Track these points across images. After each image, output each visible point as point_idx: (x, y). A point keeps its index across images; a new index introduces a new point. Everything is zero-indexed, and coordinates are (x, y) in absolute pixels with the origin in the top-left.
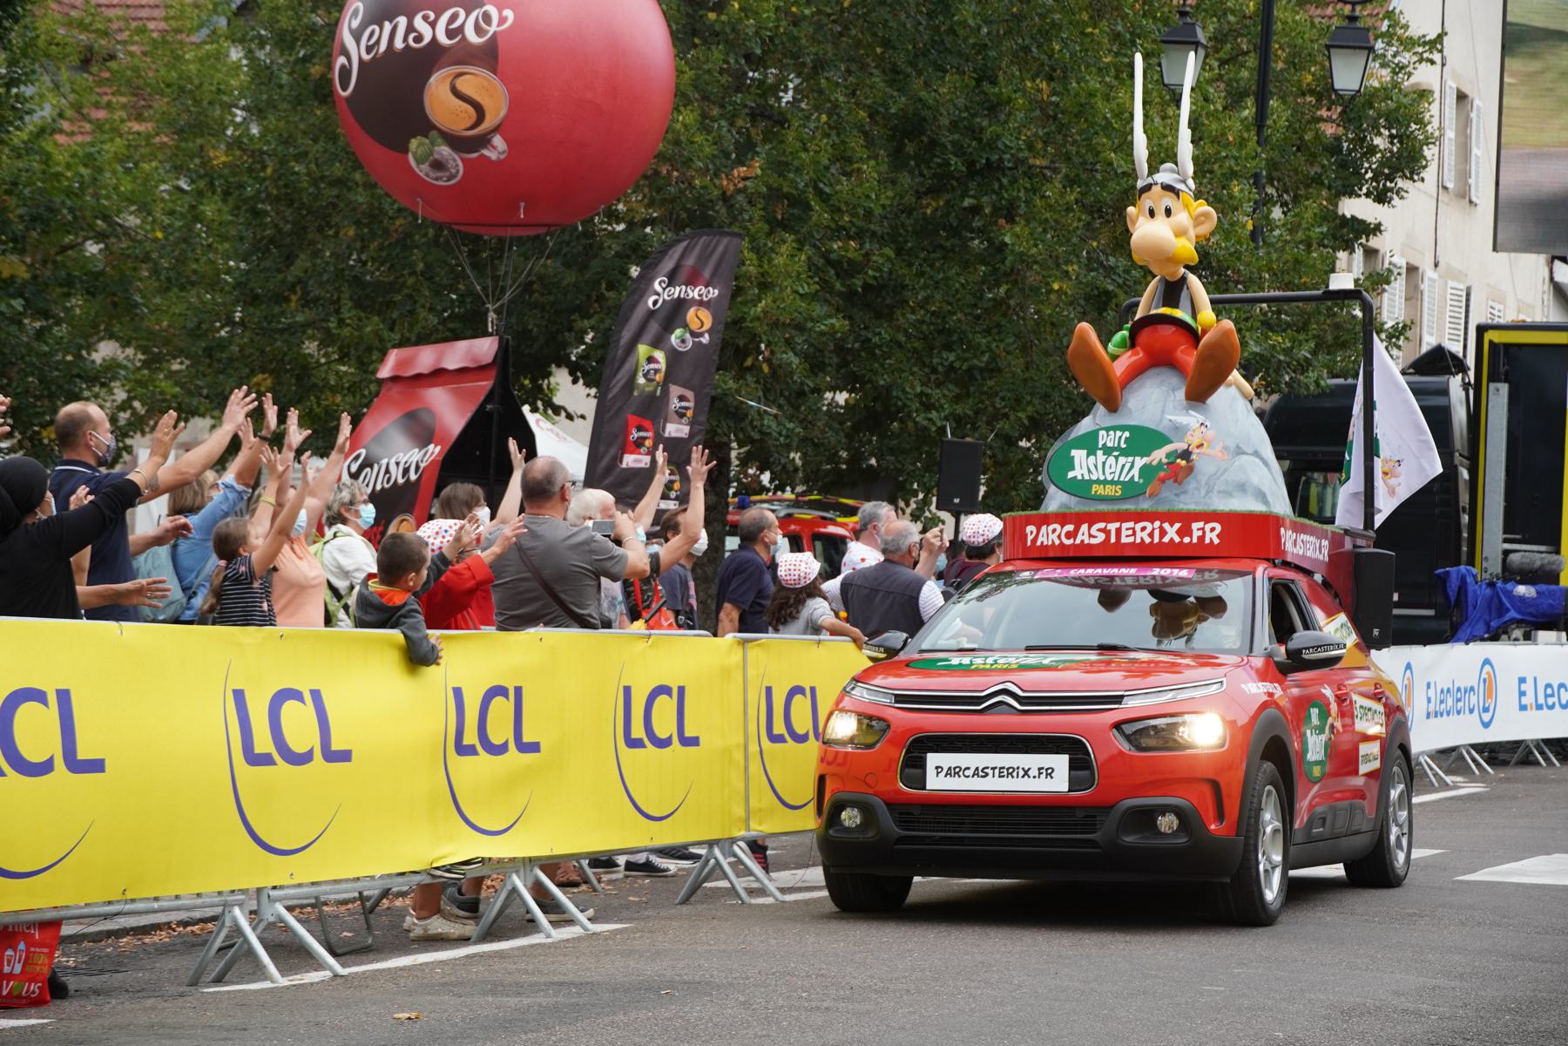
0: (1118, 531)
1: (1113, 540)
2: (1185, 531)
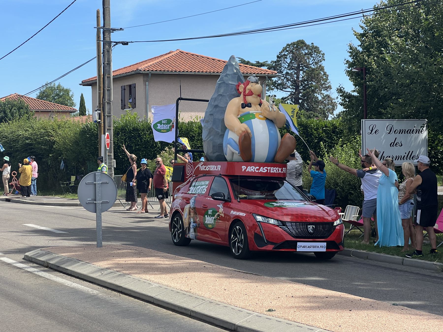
0: (270, 169)
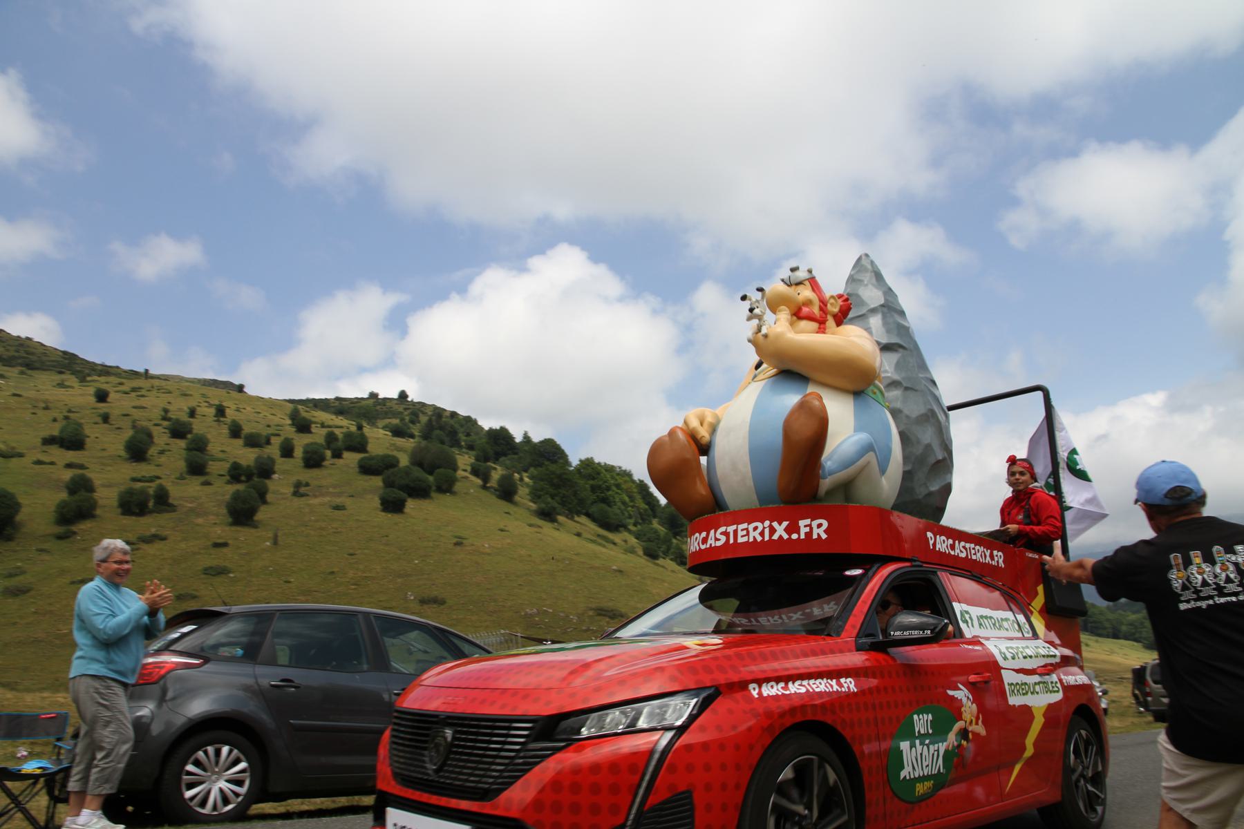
0: (736, 532)
1: (732, 541)
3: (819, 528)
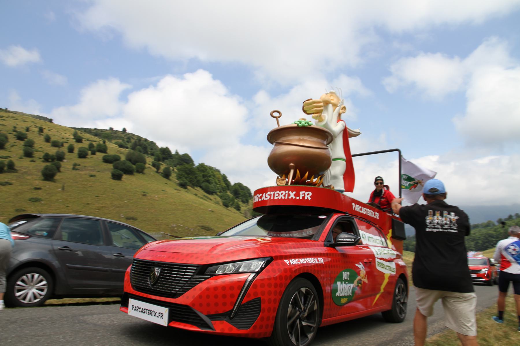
0: (274, 194)
1: (272, 198)
2: (297, 195)
3: (308, 195)
